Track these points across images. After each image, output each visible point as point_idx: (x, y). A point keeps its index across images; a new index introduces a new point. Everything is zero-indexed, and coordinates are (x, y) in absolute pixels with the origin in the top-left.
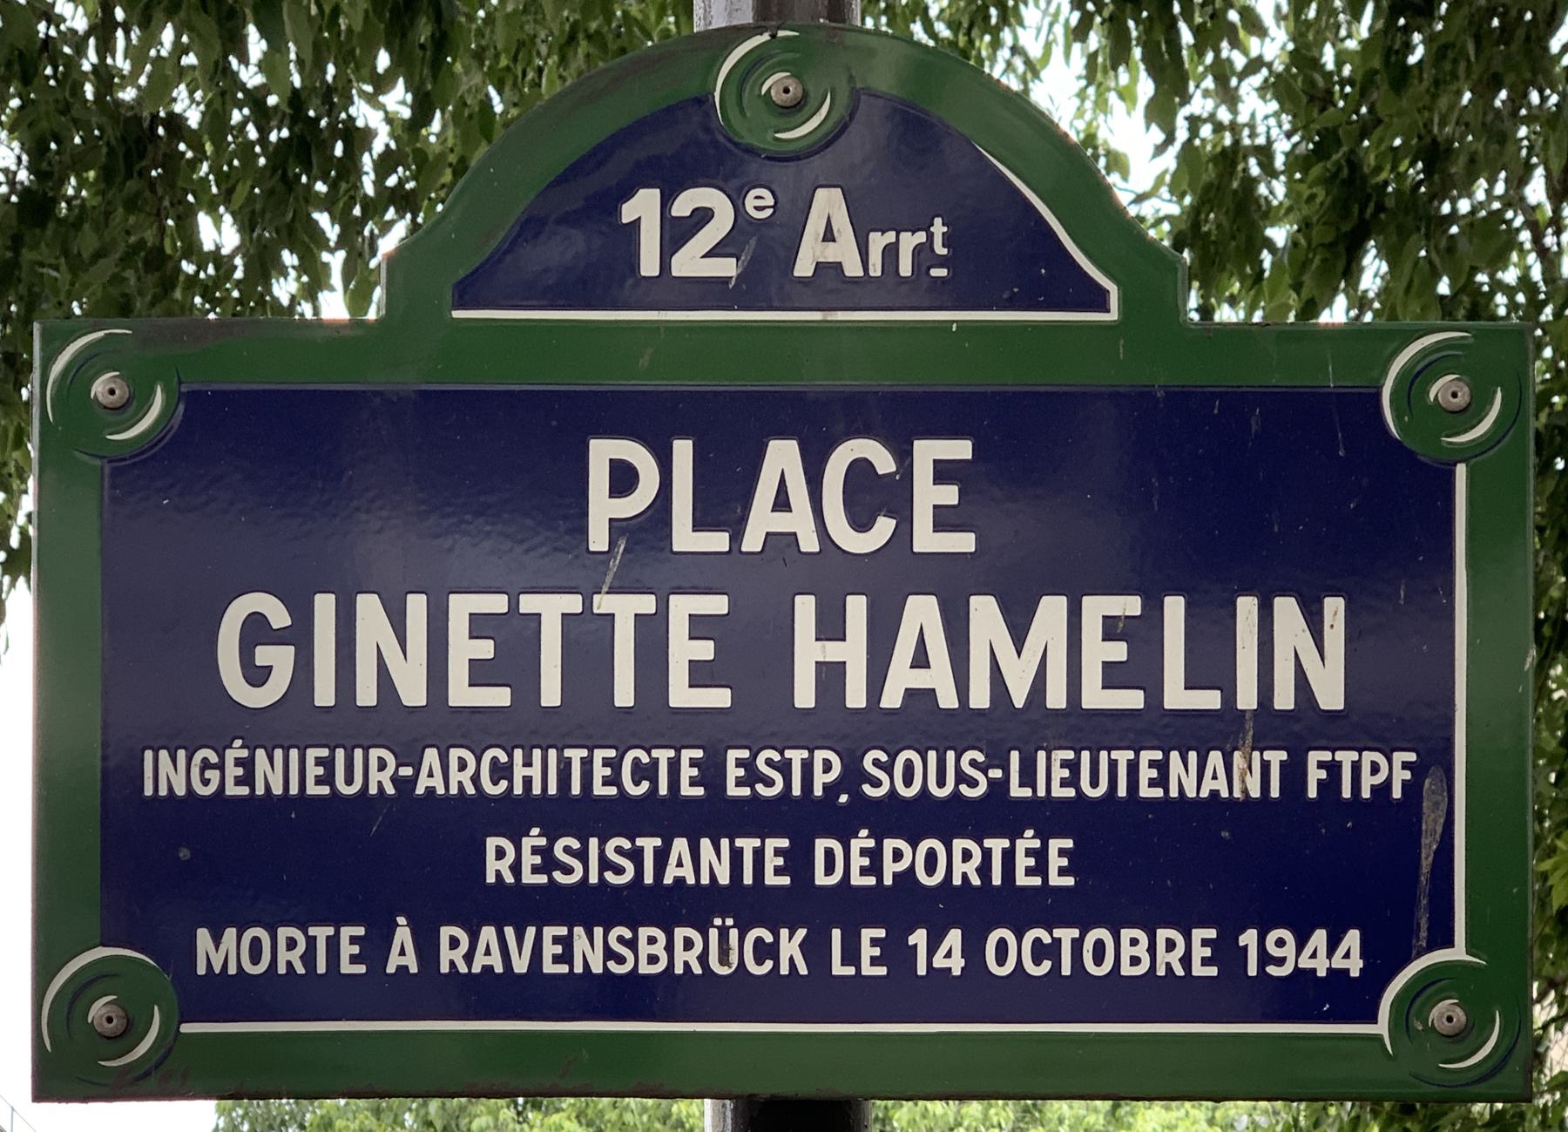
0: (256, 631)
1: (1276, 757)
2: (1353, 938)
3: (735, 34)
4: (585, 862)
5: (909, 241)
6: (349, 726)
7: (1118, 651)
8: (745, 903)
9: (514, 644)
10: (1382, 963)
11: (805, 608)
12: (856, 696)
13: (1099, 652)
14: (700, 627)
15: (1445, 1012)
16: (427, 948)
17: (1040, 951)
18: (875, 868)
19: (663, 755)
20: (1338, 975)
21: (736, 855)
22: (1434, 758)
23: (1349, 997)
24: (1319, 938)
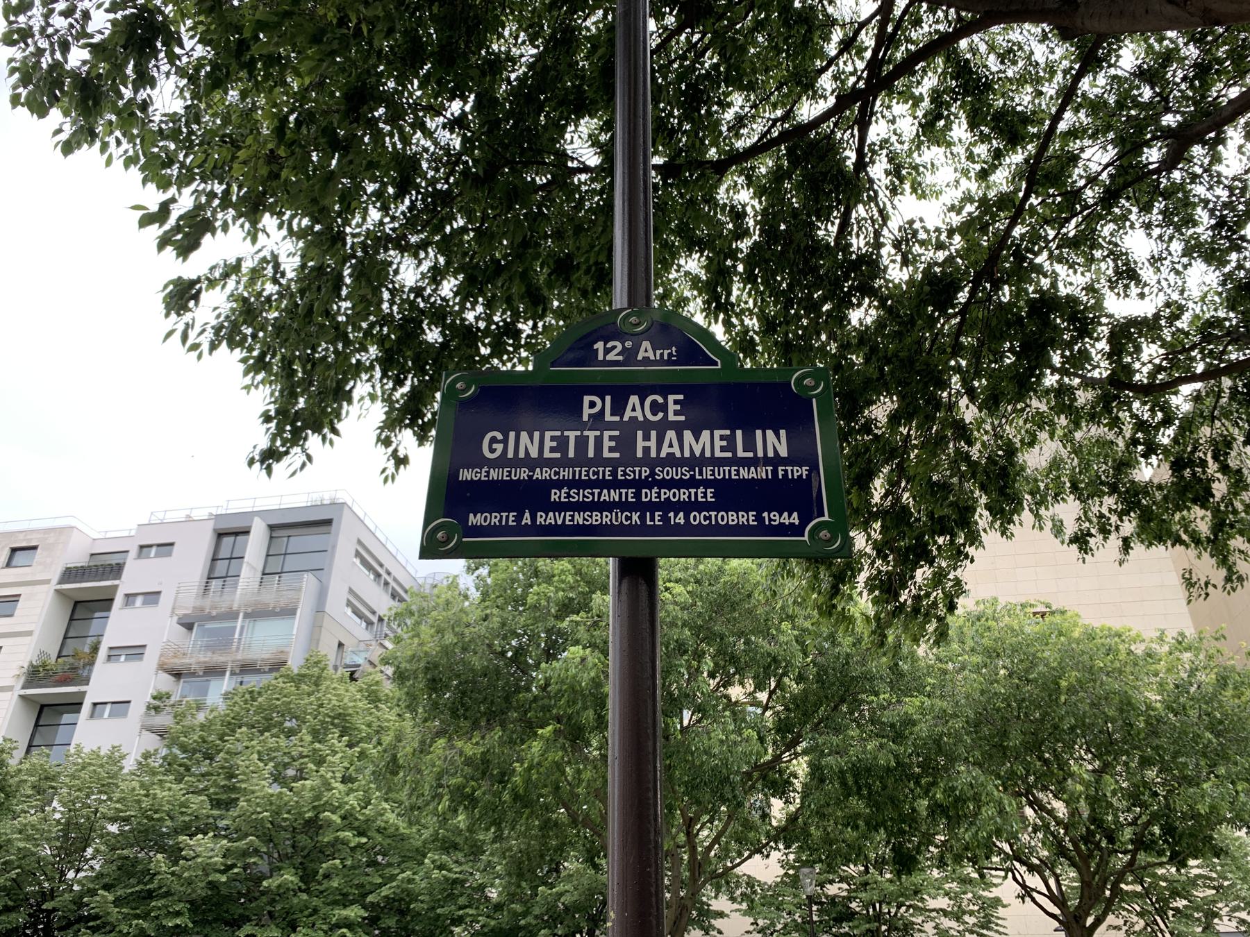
0: (494, 440)
1: (769, 468)
2: (795, 515)
3: (622, 310)
4: (577, 496)
5: (666, 352)
6: (516, 463)
7: (724, 443)
8: (623, 506)
9: (562, 444)
10: (804, 521)
11: (640, 434)
12: (653, 454)
13: (719, 443)
14: (611, 438)
15: (824, 534)
16: (533, 518)
17: (706, 518)
18: (659, 497)
19: (601, 469)
20: (792, 524)
21: (621, 494)
22: (814, 468)
23: (797, 530)
24: (786, 514)
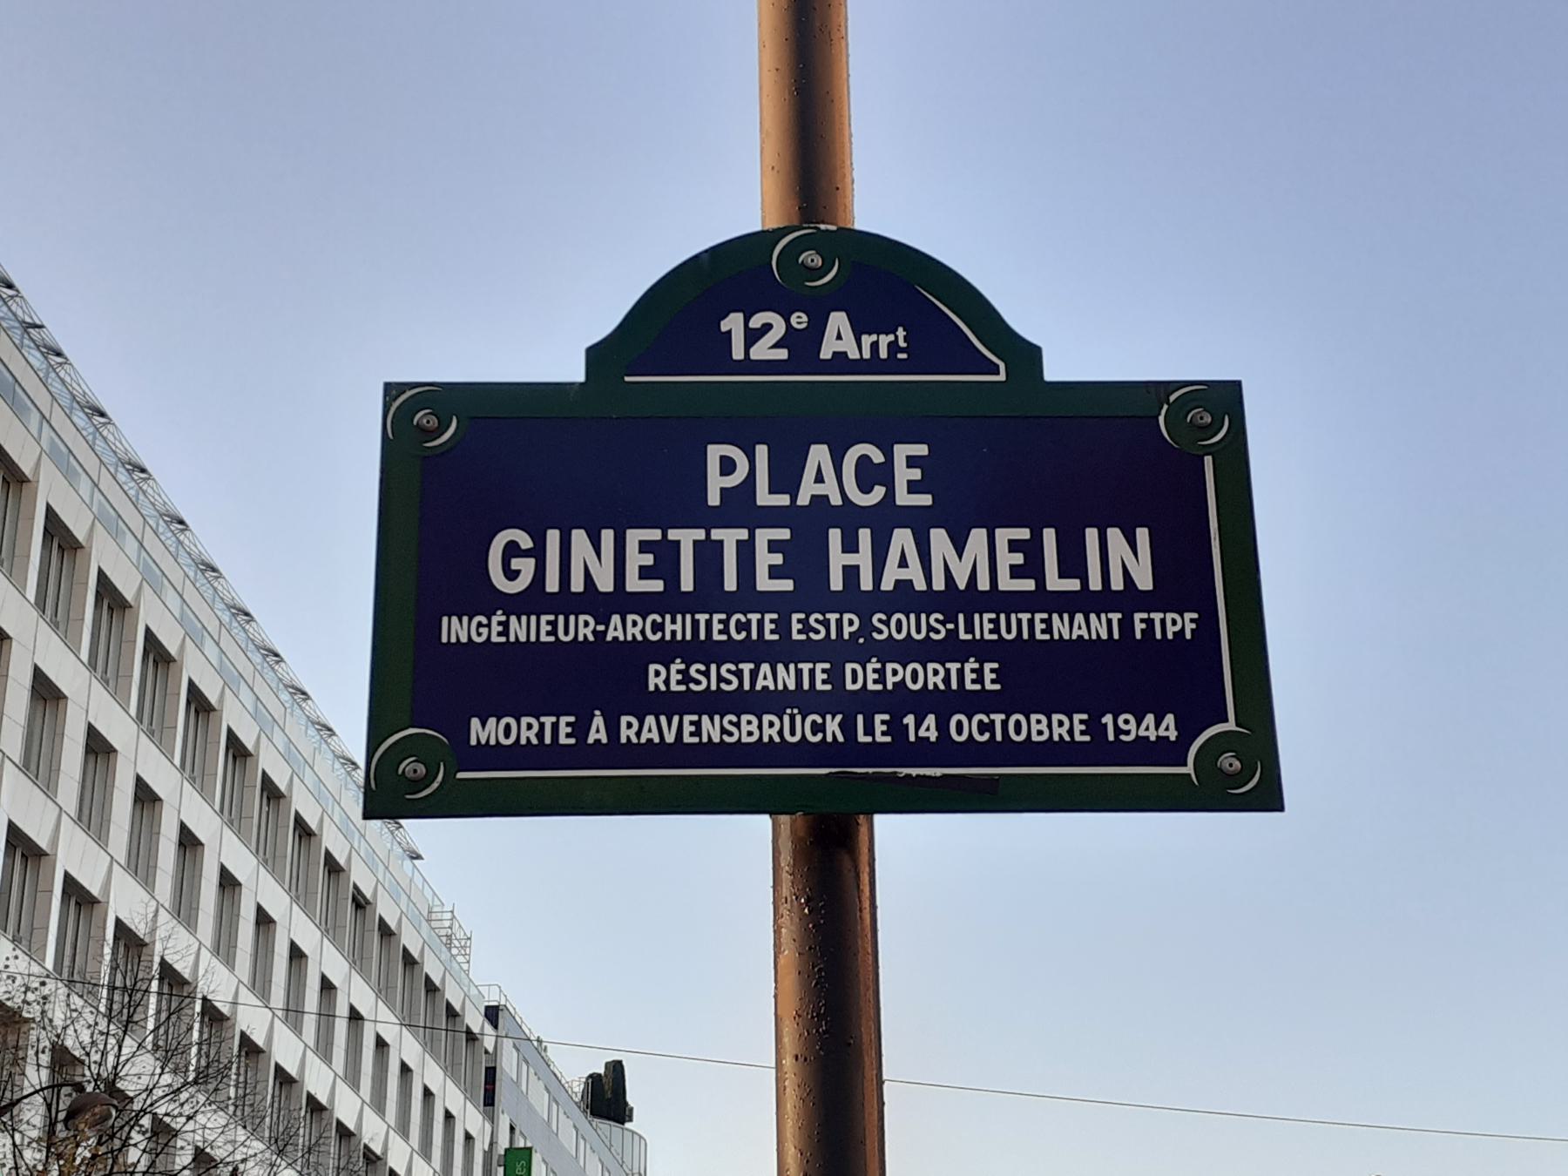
0: (512, 550)
1: (1115, 617)
6: (566, 603)
7: (1019, 559)
8: (804, 700)
9: (665, 556)
11: (835, 536)
12: (866, 584)
13: (1007, 559)
16: (613, 729)
17: (982, 728)
18: (882, 680)
19: (754, 617)
21: (799, 673)
